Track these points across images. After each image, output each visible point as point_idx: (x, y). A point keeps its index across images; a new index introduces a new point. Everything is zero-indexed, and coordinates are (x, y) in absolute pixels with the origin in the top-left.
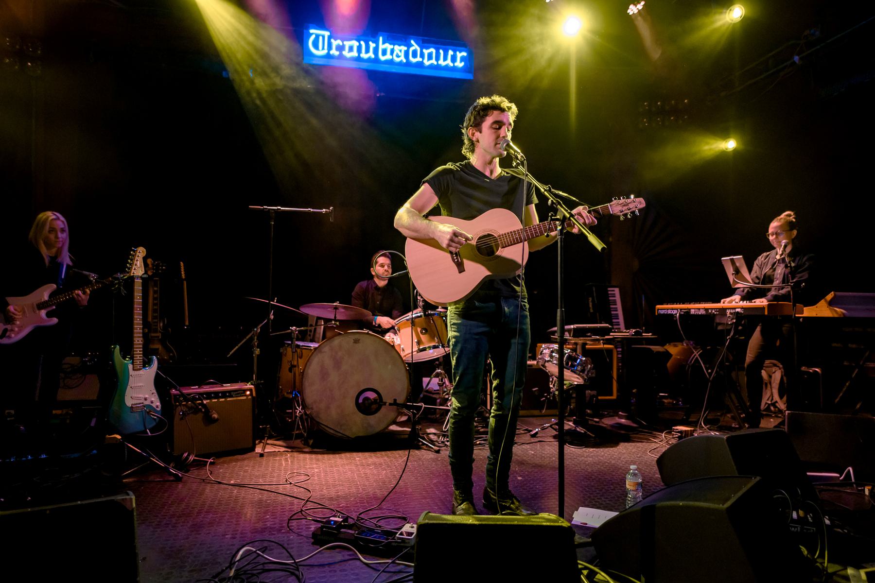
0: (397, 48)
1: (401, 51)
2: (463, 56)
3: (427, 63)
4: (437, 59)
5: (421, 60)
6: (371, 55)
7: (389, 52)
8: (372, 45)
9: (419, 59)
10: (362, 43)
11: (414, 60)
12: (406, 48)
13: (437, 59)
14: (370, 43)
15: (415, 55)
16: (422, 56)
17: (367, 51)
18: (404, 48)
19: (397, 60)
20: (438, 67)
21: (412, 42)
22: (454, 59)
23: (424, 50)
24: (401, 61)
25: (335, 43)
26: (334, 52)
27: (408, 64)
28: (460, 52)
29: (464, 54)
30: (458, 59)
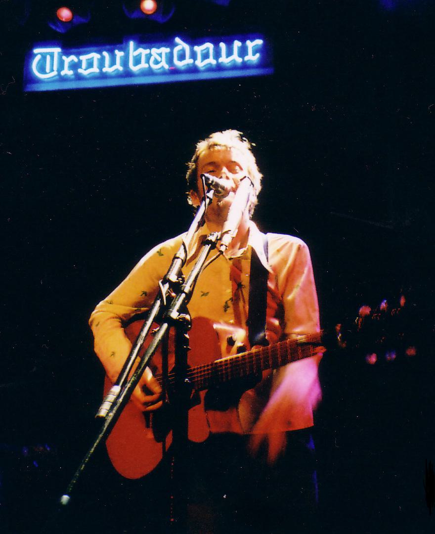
0: (154, 51)
1: (160, 55)
2: (257, 45)
3: (200, 64)
4: (217, 55)
5: (191, 61)
6: (119, 67)
7: (143, 59)
8: (119, 54)
9: (188, 61)
10: (105, 54)
11: (180, 64)
12: (168, 50)
13: (217, 55)
14: (117, 52)
15: (182, 57)
16: (194, 56)
17: (113, 63)
18: (165, 50)
19: (155, 67)
20: (220, 68)
21: (178, 40)
22: (243, 52)
23: (196, 48)
24: (163, 67)
25: (69, 60)
26: (67, 72)
27: (175, 71)
28: (252, 40)
29: (259, 42)
30: (250, 51)
